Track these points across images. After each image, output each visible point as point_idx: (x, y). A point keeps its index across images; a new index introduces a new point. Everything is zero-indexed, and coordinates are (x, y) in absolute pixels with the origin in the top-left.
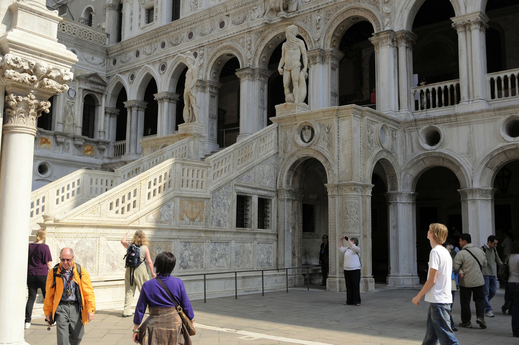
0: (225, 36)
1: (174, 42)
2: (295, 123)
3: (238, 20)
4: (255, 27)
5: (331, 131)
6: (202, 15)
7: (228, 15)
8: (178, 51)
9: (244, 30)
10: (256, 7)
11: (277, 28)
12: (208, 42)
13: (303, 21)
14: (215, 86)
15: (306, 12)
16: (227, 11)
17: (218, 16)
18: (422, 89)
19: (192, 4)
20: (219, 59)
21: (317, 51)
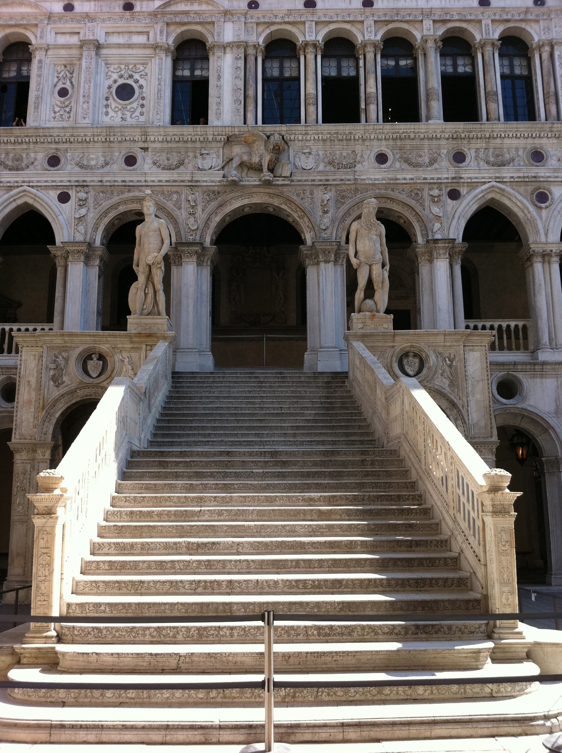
0: (138, 181)
1: (10, 163)
2: (391, 344)
3: (166, 162)
4: (206, 181)
5: (454, 364)
6: (89, 134)
7: (145, 149)
8: (24, 182)
10: (207, 152)
12: (101, 181)
13: (298, 195)
14: (105, 259)
15: (305, 183)
16: (145, 142)
17: (125, 145)
18: (476, 323)
19: (57, 109)
20: (119, 217)
21: (334, 244)
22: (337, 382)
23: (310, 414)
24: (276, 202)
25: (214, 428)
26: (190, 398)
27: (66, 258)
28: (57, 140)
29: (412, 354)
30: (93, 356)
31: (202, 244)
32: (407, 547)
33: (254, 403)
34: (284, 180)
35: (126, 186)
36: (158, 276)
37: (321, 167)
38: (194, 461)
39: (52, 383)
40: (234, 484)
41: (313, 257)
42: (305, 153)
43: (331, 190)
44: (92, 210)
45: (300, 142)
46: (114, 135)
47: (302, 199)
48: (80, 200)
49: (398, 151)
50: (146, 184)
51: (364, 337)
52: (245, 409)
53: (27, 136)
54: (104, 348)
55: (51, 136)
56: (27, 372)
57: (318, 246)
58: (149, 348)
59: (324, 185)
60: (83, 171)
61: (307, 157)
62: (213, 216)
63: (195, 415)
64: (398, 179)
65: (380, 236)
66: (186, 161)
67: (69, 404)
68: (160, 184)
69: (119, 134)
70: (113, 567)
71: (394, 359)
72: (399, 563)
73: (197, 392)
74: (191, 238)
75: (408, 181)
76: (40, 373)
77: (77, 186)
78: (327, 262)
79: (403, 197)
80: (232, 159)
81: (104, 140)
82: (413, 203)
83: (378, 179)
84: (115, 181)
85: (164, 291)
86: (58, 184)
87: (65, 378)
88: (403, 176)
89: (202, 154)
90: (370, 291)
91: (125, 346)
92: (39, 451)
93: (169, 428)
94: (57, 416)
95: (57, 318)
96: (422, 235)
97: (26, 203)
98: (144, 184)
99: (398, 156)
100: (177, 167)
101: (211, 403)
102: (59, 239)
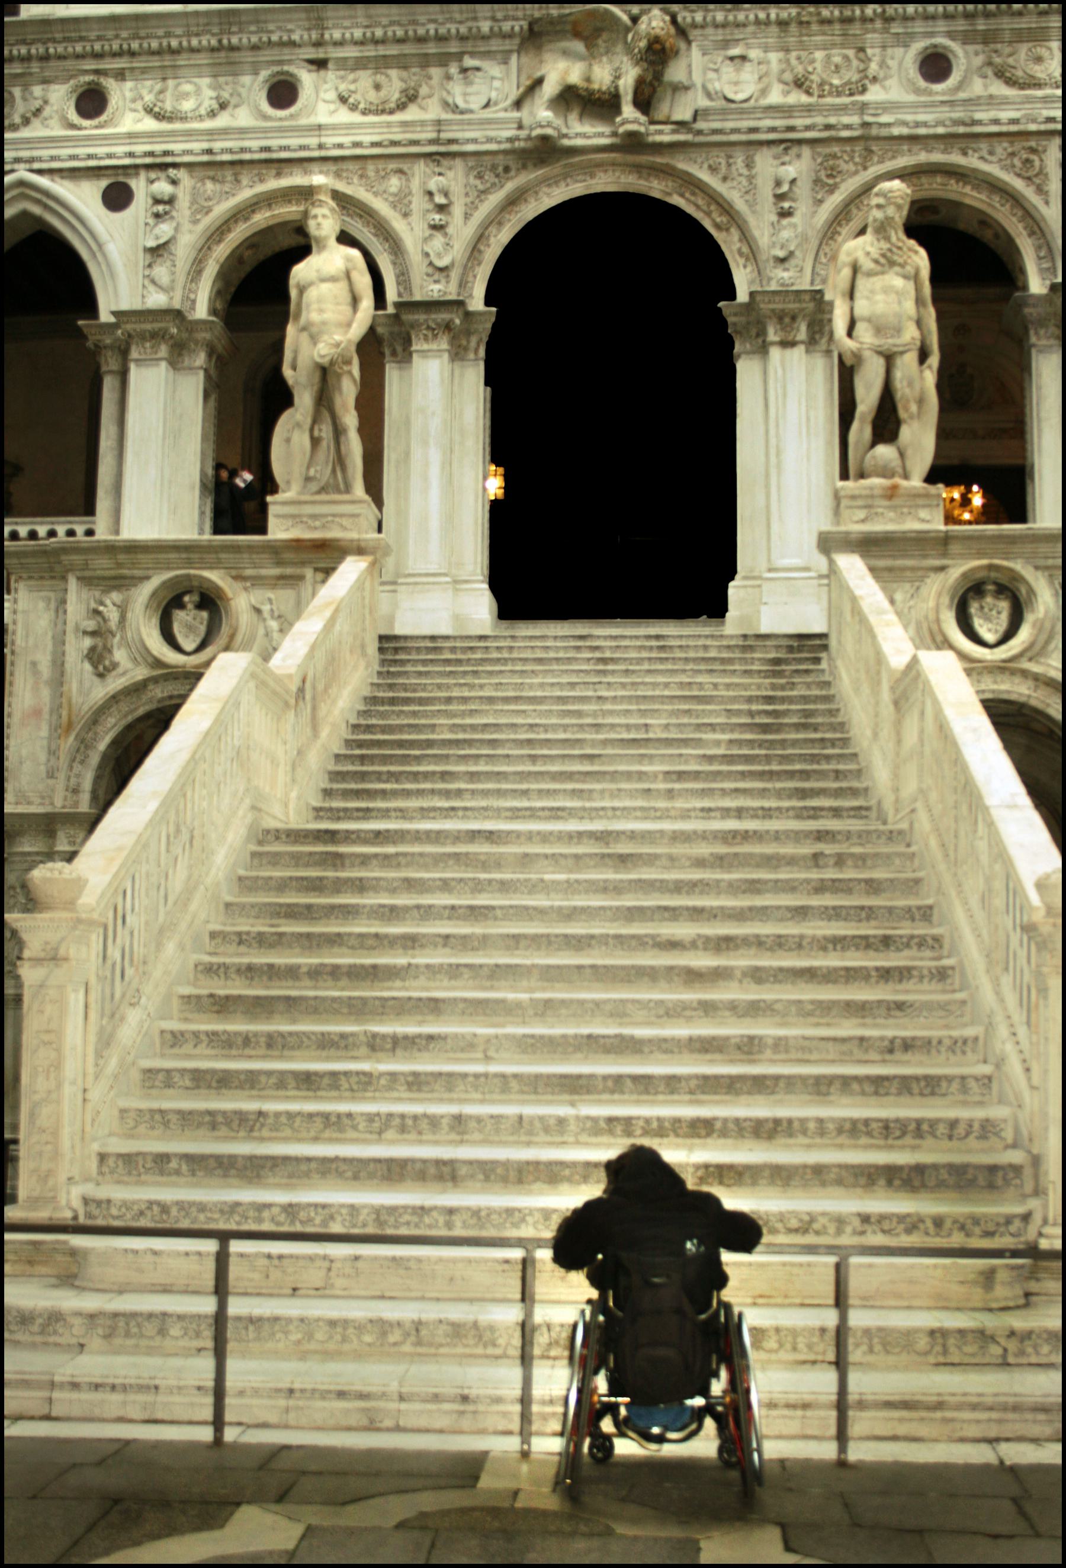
0: (303, 148)
2: (937, 563)
4: (475, 141)
6: (179, 31)
7: (320, 64)
11: (591, 170)
12: (209, 152)
13: (713, 169)
14: (220, 349)
15: (734, 138)
16: (318, 44)
17: (266, 55)
22: (800, 661)
23: (718, 742)
24: (656, 188)
25: (473, 776)
26: (421, 701)
27: (124, 353)
28: (97, 47)
29: (991, 587)
30: (186, 599)
31: (460, 304)
32: (882, 1052)
33: (579, 714)
34: (674, 132)
36: (348, 391)
37: (775, 97)
38: (405, 855)
39: (87, 667)
40: (493, 908)
41: (753, 332)
42: (732, 59)
43: (799, 156)
44: (186, 226)
45: (720, 31)
46: (241, 31)
47: (725, 179)
48: (157, 201)
49: (979, 47)
50: (323, 153)
51: (868, 546)
52: (554, 728)
53: (24, 42)
54: (214, 576)
55: (82, 39)
56: (31, 642)
57: (765, 307)
58: (320, 576)
59: (782, 141)
60: (165, 126)
61: (738, 70)
62: (493, 230)
63: (430, 744)
64: (979, 123)
65: (916, 278)
66: (424, 90)
67: (130, 718)
68: (358, 151)
69: (253, 28)
70: (200, 1079)
71: (946, 600)
72: (855, 1086)
73: (439, 687)
74: (436, 287)
75: (1004, 129)
76: (60, 641)
77: (149, 167)
78: (787, 344)
79: (993, 169)
80: (539, 82)
81: (214, 42)
82: (1018, 184)
83: (925, 124)
84: (243, 150)
85: (361, 430)
86: (103, 163)
87: (120, 655)
88: (992, 114)
89: (464, 70)
90: (887, 424)
91: (264, 572)
93: (363, 776)
94: (102, 746)
95: (103, 503)
96: (1041, 271)
98: (316, 154)
99: (979, 60)
100: (401, 107)
101: (472, 713)
102: (107, 306)
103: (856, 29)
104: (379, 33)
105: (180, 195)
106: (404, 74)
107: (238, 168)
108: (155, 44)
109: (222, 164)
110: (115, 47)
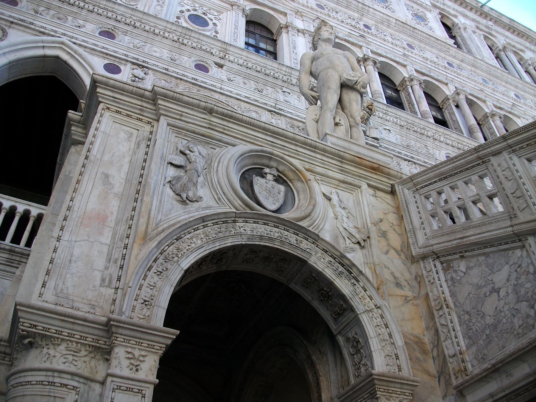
7: (221, 66)
8: (64, 35)
9: (266, 104)
17: (198, 52)
28: (119, 18)
35: (196, 85)
50: (222, 91)
55: (112, 11)
56: (106, 158)
67: (217, 246)
69: (196, 40)
86: (109, 53)
91: (330, 173)
92: (120, 352)
94: (186, 263)
97: (57, 58)
98: (219, 90)
103: (424, 138)
104: (250, 65)
105: (148, 79)
106: (257, 84)
107: (179, 81)
108: (147, 28)
109: (172, 76)
110: (128, 21)
